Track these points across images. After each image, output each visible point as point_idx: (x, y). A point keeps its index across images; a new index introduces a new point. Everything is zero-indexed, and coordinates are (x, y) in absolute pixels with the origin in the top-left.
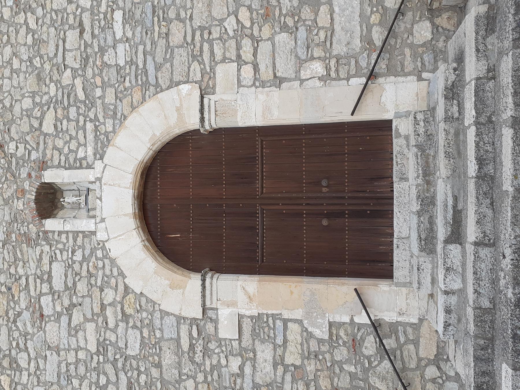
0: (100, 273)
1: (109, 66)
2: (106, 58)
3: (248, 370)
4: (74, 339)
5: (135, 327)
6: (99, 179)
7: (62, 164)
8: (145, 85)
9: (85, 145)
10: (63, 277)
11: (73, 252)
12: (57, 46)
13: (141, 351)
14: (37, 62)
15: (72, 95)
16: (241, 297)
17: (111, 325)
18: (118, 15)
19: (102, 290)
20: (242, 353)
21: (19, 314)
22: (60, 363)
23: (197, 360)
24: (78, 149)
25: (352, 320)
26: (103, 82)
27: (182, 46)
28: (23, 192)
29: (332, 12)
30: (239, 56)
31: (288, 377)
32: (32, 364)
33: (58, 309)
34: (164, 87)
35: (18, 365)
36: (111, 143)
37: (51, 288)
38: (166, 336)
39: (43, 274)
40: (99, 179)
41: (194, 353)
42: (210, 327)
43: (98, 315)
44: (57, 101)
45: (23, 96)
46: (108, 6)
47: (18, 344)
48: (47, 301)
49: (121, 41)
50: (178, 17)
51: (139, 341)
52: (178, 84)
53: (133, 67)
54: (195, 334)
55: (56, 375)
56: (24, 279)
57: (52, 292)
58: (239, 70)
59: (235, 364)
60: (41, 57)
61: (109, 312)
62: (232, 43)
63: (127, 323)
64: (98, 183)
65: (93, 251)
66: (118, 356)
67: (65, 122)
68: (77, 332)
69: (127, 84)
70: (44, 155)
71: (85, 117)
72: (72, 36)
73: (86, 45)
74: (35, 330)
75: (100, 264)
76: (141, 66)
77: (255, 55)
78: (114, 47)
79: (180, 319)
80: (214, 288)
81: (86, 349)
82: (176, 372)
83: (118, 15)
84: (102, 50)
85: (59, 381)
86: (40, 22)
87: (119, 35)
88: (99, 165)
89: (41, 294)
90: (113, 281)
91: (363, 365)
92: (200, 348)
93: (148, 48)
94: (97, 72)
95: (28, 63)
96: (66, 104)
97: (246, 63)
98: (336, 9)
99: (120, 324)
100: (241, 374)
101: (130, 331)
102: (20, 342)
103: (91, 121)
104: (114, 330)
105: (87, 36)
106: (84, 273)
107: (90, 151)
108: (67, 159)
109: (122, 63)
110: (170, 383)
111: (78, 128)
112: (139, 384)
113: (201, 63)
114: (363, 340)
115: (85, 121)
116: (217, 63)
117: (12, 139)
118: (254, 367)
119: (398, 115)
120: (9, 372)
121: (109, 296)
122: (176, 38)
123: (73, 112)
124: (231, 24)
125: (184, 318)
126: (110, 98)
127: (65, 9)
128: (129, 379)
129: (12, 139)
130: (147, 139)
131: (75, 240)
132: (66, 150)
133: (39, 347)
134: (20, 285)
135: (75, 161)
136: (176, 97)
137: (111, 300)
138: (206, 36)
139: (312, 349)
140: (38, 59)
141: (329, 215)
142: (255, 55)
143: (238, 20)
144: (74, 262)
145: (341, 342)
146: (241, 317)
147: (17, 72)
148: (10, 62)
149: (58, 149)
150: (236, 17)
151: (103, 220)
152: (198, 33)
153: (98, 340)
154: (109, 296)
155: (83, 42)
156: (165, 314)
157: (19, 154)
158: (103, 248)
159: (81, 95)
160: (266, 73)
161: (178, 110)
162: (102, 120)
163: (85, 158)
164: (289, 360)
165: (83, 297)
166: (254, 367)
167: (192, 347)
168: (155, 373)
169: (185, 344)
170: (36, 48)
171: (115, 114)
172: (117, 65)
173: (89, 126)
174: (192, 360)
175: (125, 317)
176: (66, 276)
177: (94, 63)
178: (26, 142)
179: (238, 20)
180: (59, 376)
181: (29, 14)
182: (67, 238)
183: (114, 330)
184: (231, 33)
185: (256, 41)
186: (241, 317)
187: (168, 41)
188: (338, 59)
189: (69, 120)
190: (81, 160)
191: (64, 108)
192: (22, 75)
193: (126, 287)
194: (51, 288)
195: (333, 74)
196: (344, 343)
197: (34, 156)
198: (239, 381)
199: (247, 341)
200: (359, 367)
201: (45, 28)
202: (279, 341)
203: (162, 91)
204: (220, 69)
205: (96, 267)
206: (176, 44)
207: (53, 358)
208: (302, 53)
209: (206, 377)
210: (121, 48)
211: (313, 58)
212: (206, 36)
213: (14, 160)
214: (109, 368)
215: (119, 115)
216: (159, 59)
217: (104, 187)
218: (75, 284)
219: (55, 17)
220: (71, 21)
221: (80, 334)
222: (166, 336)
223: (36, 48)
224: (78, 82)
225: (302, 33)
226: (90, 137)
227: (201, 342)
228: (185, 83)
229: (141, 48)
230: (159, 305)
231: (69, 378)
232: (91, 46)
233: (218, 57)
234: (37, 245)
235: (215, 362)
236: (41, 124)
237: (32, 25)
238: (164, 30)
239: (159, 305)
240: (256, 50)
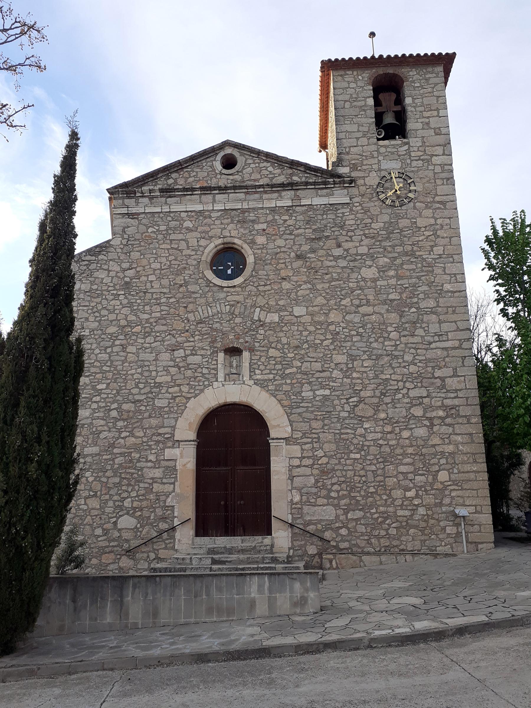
0: (197, 384)
1: (302, 387)
2: (306, 385)
3: (149, 464)
4: (162, 369)
5: (169, 403)
6: (244, 383)
7: (252, 361)
8: (291, 407)
9: (262, 374)
10: (194, 363)
11: (207, 368)
12: (313, 358)
13: (157, 407)
14: (306, 346)
15: (288, 366)
16: (185, 460)
17: (170, 390)
18: (327, 392)
19: (187, 384)
20: (158, 461)
21: (174, 337)
22: (149, 361)
23: (154, 437)
24: (260, 370)
25: (176, 517)
26: (294, 384)
27: (310, 427)
28: (238, 339)
29: (323, 505)
30: (304, 458)
31: (147, 485)
32: (148, 345)
33: (177, 360)
34: (290, 417)
35: (147, 337)
36: (263, 389)
37: (188, 355)
38: (165, 420)
39: (195, 351)
40: (244, 383)
41: (157, 436)
42: (170, 444)
43: (175, 383)
44: (285, 357)
45: (288, 338)
46: (332, 386)
47: (158, 336)
48: (180, 353)
49: (314, 393)
50: (325, 425)
51: (162, 406)
52: (291, 425)
53: (300, 401)
54: (166, 436)
55: (143, 359)
56: (192, 339)
57: (186, 356)
58: (297, 458)
59: (152, 458)
60: (308, 348)
61: (177, 389)
62: (311, 455)
63: (171, 399)
64: (242, 382)
65: (208, 379)
66: (154, 394)
67: (274, 362)
68: (166, 371)
69: (292, 397)
70: (257, 351)
71: (276, 374)
72: (318, 366)
73: (313, 374)
74: (166, 347)
75: (201, 384)
76: (301, 405)
77: (304, 466)
78: (311, 390)
79: (174, 428)
80: (189, 446)
81: (157, 376)
82: (147, 426)
83: (327, 392)
84: (310, 383)
85: (140, 361)
86: (327, 348)
87: (317, 393)
88: (252, 382)
89: (185, 350)
90: (193, 391)
91: (154, 523)
92: (160, 439)
93: (310, 409)
94: (299, 380)
95: (305, 341)
96: (283, 363)
97: (301, 461)
98: (325, 508)
99: (171, 395)
100: (147, 461)
101: (168, 401)
102: (159, 338)
103: (274, 377)
104: (167, 392)
105: (318, 375)
106: (196, 374)
107: (259, 377)
108: (255, 364)
109: (303, 394)
110: (141, 423)
111: (271, 370)
112: (140, 406)
113: (302, 438)
114: (166, 522)
115: (274, 374)
116: (301, 446)
117: (266, 331)
118: (151, 468)
119: (273, 538)
120: (143, 331)
121: (185, 389)
122: (315, 424)
123: (279, 367)
124: (320, 453)
125: (174, 430)
126: (286, 388)
127: (332, 362)
128: (142, 400)
129: (266, 331)
130: (264, 409)
131: (213, 369)
132: (259, 363)
133: (158, 349)
134: (189, 337)
135: (254, 368)
136: (285, 424)
137: (183, 390)
138: (314, 440)
139: (161, 497)
140: (307, 346)
141: (226, 505)
142: (304, 466)
143: (322, 457)
144: (202, 368)
145: (165, 512)
146: (175, 460)
147: (301, 334)
148: (306, 330)
149: (260, 358)
150: (323, 456)
151: (223, 385)
152: (316, 436)
153: (162, 383)
154: (185, 389)
155: (315, 372)
156: (176, 420)
157: (257, 336)
158: (209, 385)
159: (287, 371)
160: (296, 472)
161: (278, 425)
162: (274, 383)
163: (255, 374)
164: (155, 485)
165: (184, 374)
166: (151, 468)
167: (160, 434)
168: (146, 415)
169: (161, 431)
170: (313, 345)
171: (278, 391)
172: (302, 392)
173: (271, 376)
174: (153, 435)
175: (174, 398)
176: (195, 364)
177: (304, 379)
178: (264, 340)
179: (322, 457)
180: (142, 361)
181: (331, 341)
182: (214, 364)
183: (167, 392)
184: (315, 453)
185: (311, 466)
186: (175, 460)
187: (313, 419)
188: (301, 509)
189: (275, 365)
190: (254, 371)
191: (281, 362)
192: (298, 337)
193: (189, 398)
194: (188, 355)
195: (294, 506)
196: (165, 513)
197: (257, 344)
198: (144, 460)
199: (163, 463)
200: (153, 521)
201: (323, 350)
202: (164, 481)
203: (288, 416)
204: (298, 447)
205: (199, 381)
206: (312, 424)
207: (152, 356)
208: (304, 490)
209: (145, 442)
210: (310, 394)
211: (302, 496)
212: (314, 440)
213: (255, 333)
214: (147, 389)
215: (277, 393)
216: (304, 415)
217: (240, 386)
218: (191, 369)
219: (328, 356)
220: (326, 366)
221: (165, 373)
222: (165, 420)
223: (313, 345)
224: (295, 370)
225: (314, 490)
226: (266, 377)
227: (163, 439)
228: (292, 428)
229: (310, 405)
230: (181, 417)
231: (141, 367)
232: (312, 377)
233: (304, 447)
234: (210, 347)
235: (153, 447)
236: (273, 348)
237: (325, 343)
238: (319, 418)
239: (181, 417)
240: (307, 466)
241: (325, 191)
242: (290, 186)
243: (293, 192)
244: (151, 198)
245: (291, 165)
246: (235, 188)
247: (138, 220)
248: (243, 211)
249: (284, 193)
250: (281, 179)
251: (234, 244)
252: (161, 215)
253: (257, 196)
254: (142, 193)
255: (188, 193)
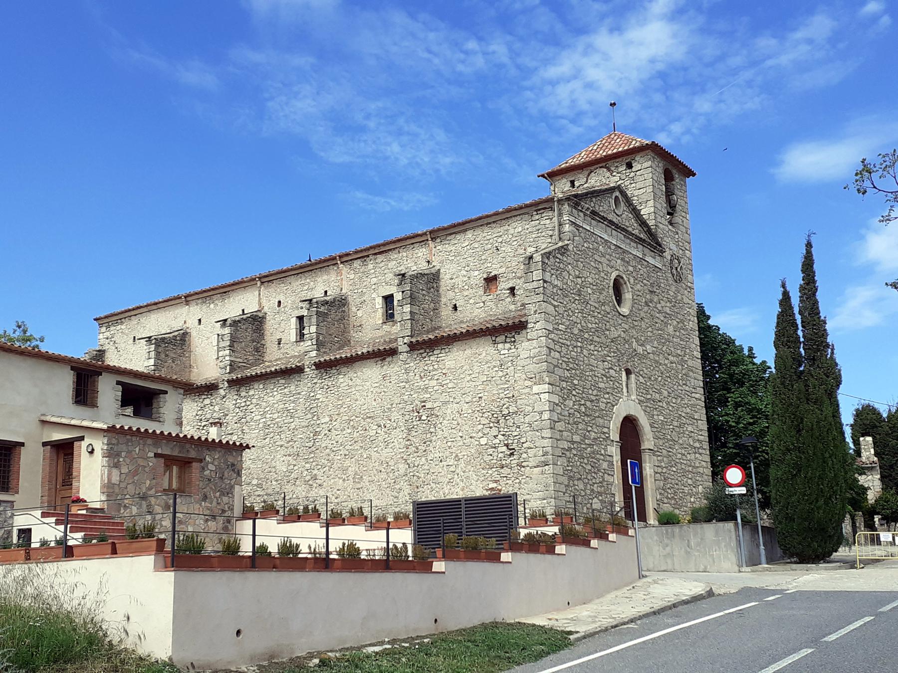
241: (653, 253)
242: (641, 241)
243: (642, 247)
244: (585, 215)
245: (642, 224)
246: (623, 230)
247: (579, 233)
248: (624, 251)
249: (639, 246)
250: (636, 232)
251: (622, 278)
252: (589, 233)
253: (628, 241)
254: (582, 208)
255: (602, 221)
